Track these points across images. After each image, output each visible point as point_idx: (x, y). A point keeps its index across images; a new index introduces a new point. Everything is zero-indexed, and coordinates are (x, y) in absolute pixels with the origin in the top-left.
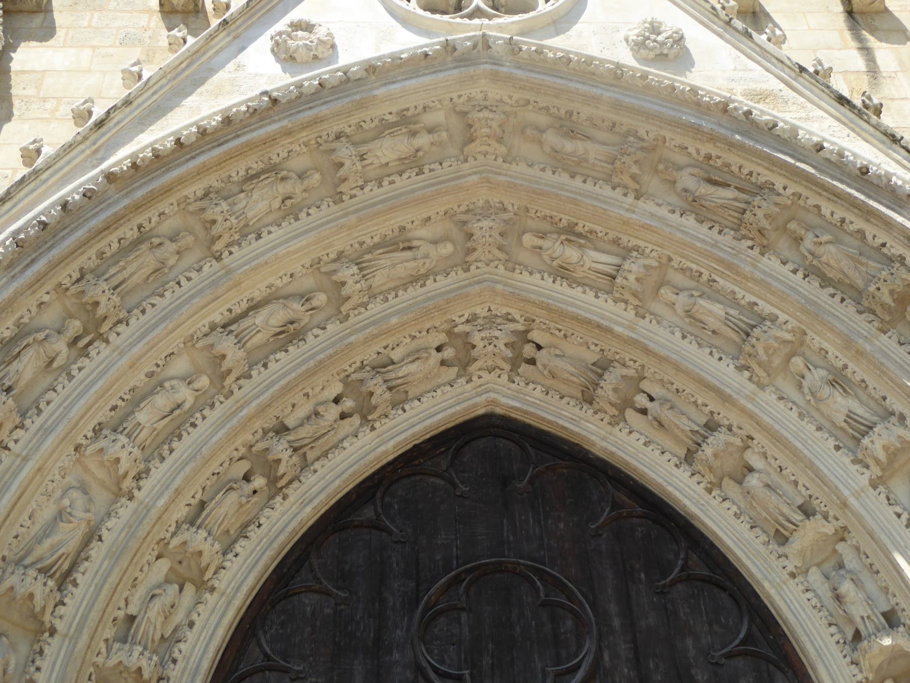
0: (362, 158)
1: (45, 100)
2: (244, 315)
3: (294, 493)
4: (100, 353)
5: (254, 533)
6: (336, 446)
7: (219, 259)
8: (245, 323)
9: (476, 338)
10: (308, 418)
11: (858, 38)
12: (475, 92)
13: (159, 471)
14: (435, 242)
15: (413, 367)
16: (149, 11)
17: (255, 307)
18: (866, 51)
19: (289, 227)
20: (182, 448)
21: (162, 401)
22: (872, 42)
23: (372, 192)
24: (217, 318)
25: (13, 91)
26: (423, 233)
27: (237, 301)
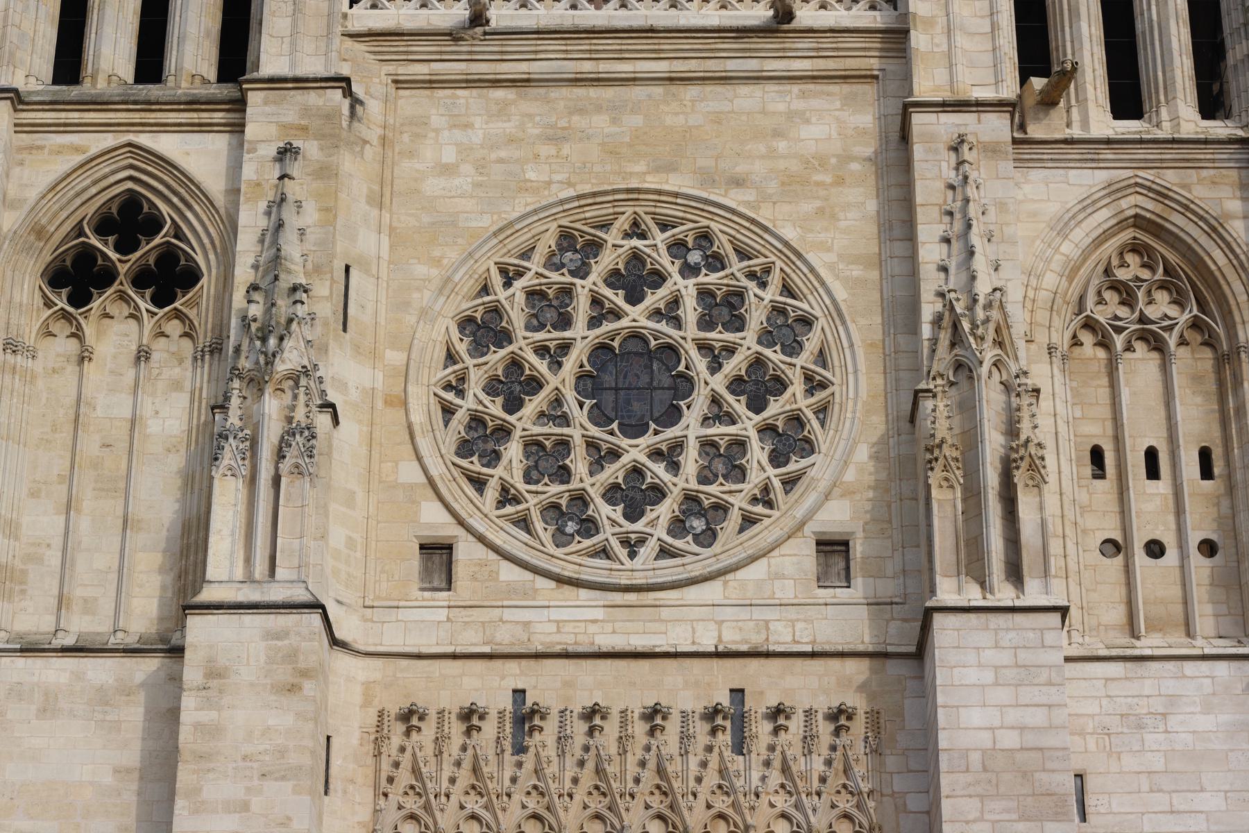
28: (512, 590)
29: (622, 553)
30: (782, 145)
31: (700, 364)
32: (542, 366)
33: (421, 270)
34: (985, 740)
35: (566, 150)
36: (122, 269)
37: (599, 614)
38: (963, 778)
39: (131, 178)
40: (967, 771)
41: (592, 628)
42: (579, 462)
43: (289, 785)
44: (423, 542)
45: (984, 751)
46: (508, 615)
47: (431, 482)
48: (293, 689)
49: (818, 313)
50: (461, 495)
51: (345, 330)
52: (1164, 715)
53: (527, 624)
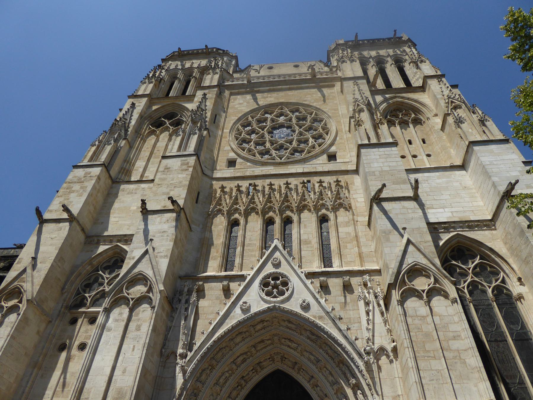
0: (254, 329)
1: (204, 314)
2: (236, 359)
3: (245, 388)
4: (214, 371)
5: (239, 396)
6: (252, 378)
7: (232, 350)
8: (237, 360)
9: (275, 357)
10: (247, 374)
11: (344, 293)
12: (274, 315)
13: (224, 389)
14: (268, 340)
15: (264, 363)
16: (220, 290)
17: (238, 357)
18: (345, 296)
19: (243, 342)
20: (227, 384)
21: (224, 377)
22: (347, 294)
23: (257, 334)
24: (232, 361)
25: (199, 312)
26: (266, 338)
27: (235, 357)
28: (250, 166)
29: (278, 159)
30: (314, 95)
31: (297, 128)
32: (260, 130)
33: (233, 118)
34: (380, 169)
35: (267, 99)
36: (168, 123)
37: (273, 168)
38: (374, 177)
39: (173, 110)
40: (375, 175)
41: (270, 171)
42: (268, 145)
43: (182, 188)
44: (229, 160)
45: (379, 171)
46: (248, 169)
47: (232, 149)
48: (186, 170)
49: (324, 117)
50: (240, 152)
51: (214, 123)
52: (427, 180)
53: (253, 171)
